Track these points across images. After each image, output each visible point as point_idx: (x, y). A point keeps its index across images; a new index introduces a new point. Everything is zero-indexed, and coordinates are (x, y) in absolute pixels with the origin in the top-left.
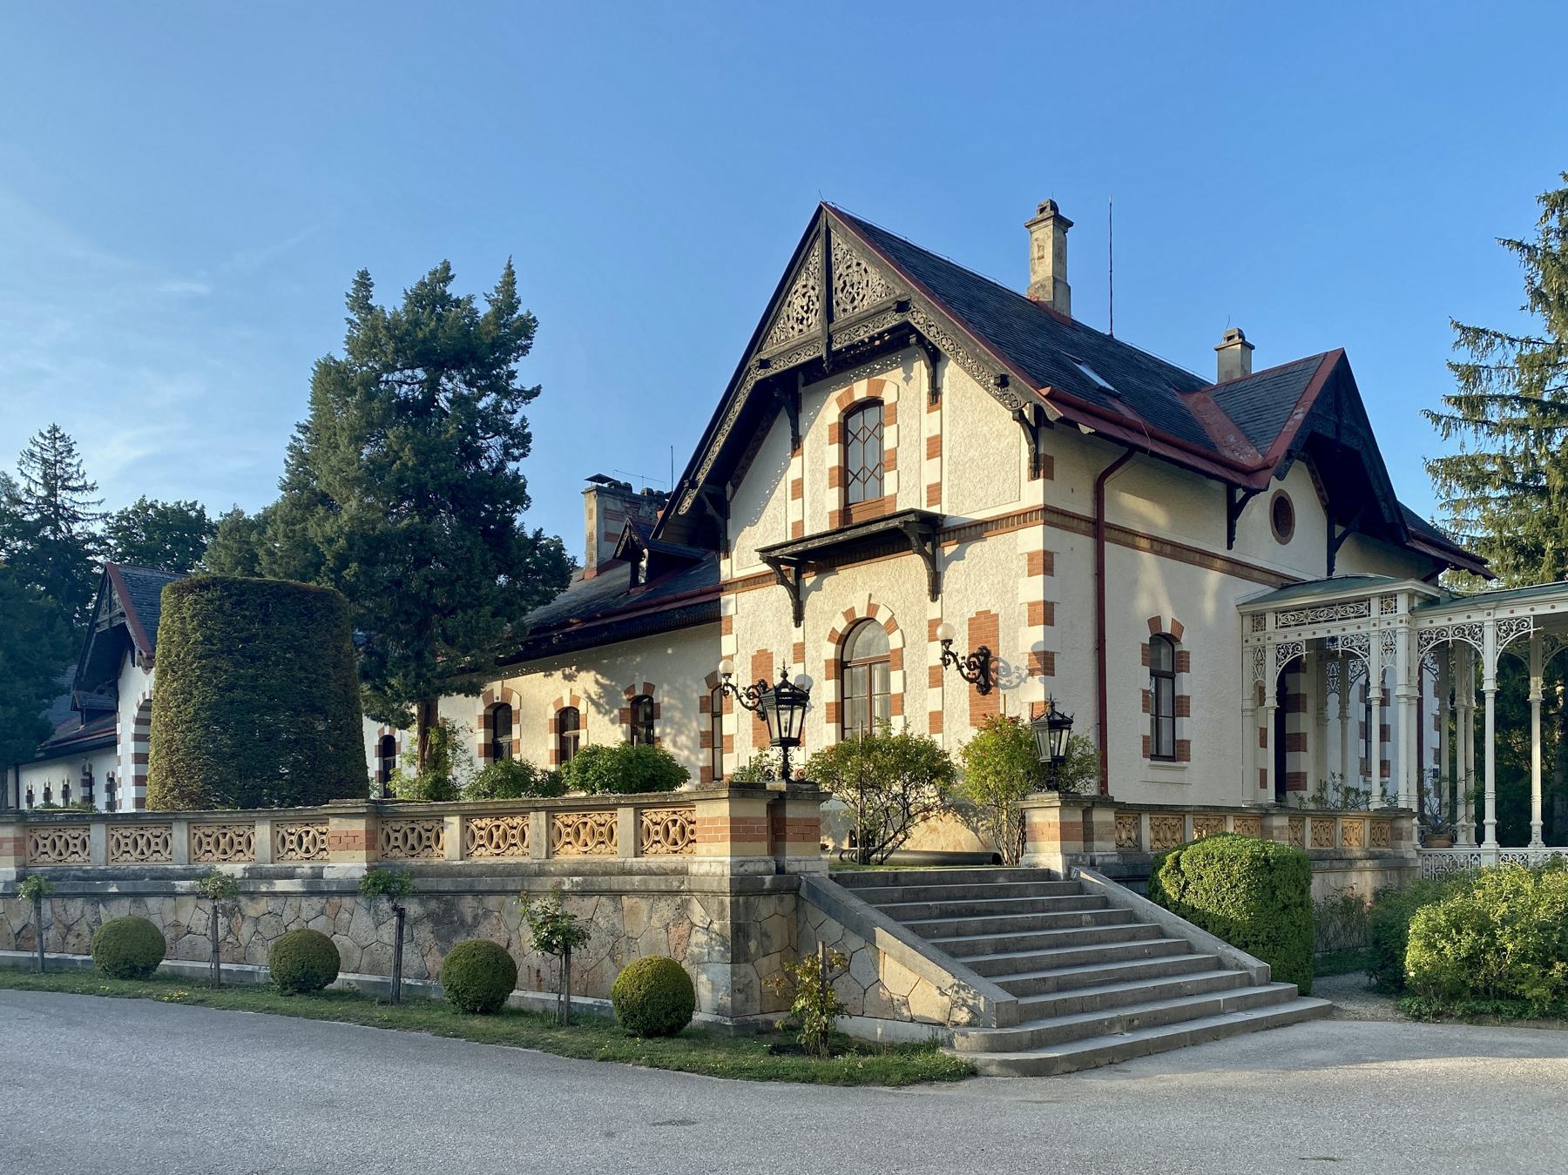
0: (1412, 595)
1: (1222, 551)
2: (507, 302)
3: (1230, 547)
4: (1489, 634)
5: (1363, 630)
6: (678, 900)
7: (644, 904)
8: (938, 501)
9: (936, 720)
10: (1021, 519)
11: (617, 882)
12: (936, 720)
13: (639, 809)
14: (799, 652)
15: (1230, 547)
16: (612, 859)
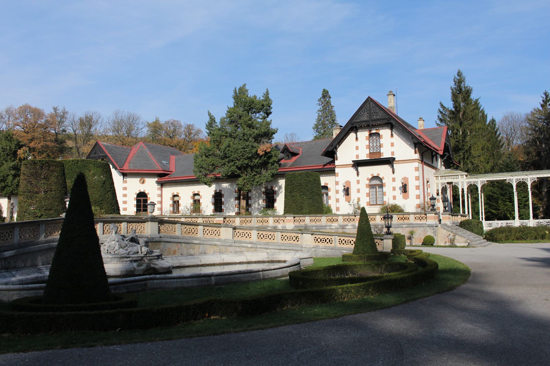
0: (466, 175)
1: (431, 164)
2: (267, 94)
3: (432, 163)
4: (479, 183)
5: (458, 181)
6: (424, 228)
7: (418, 228)
8: (394, 155)
9: (394, 198)
10: (413, 160)
11: (413, 226)
12: (394, 198)
13: (379, 214)
14: (358, 182)
15: (432, 163)
16: (409, 222)
